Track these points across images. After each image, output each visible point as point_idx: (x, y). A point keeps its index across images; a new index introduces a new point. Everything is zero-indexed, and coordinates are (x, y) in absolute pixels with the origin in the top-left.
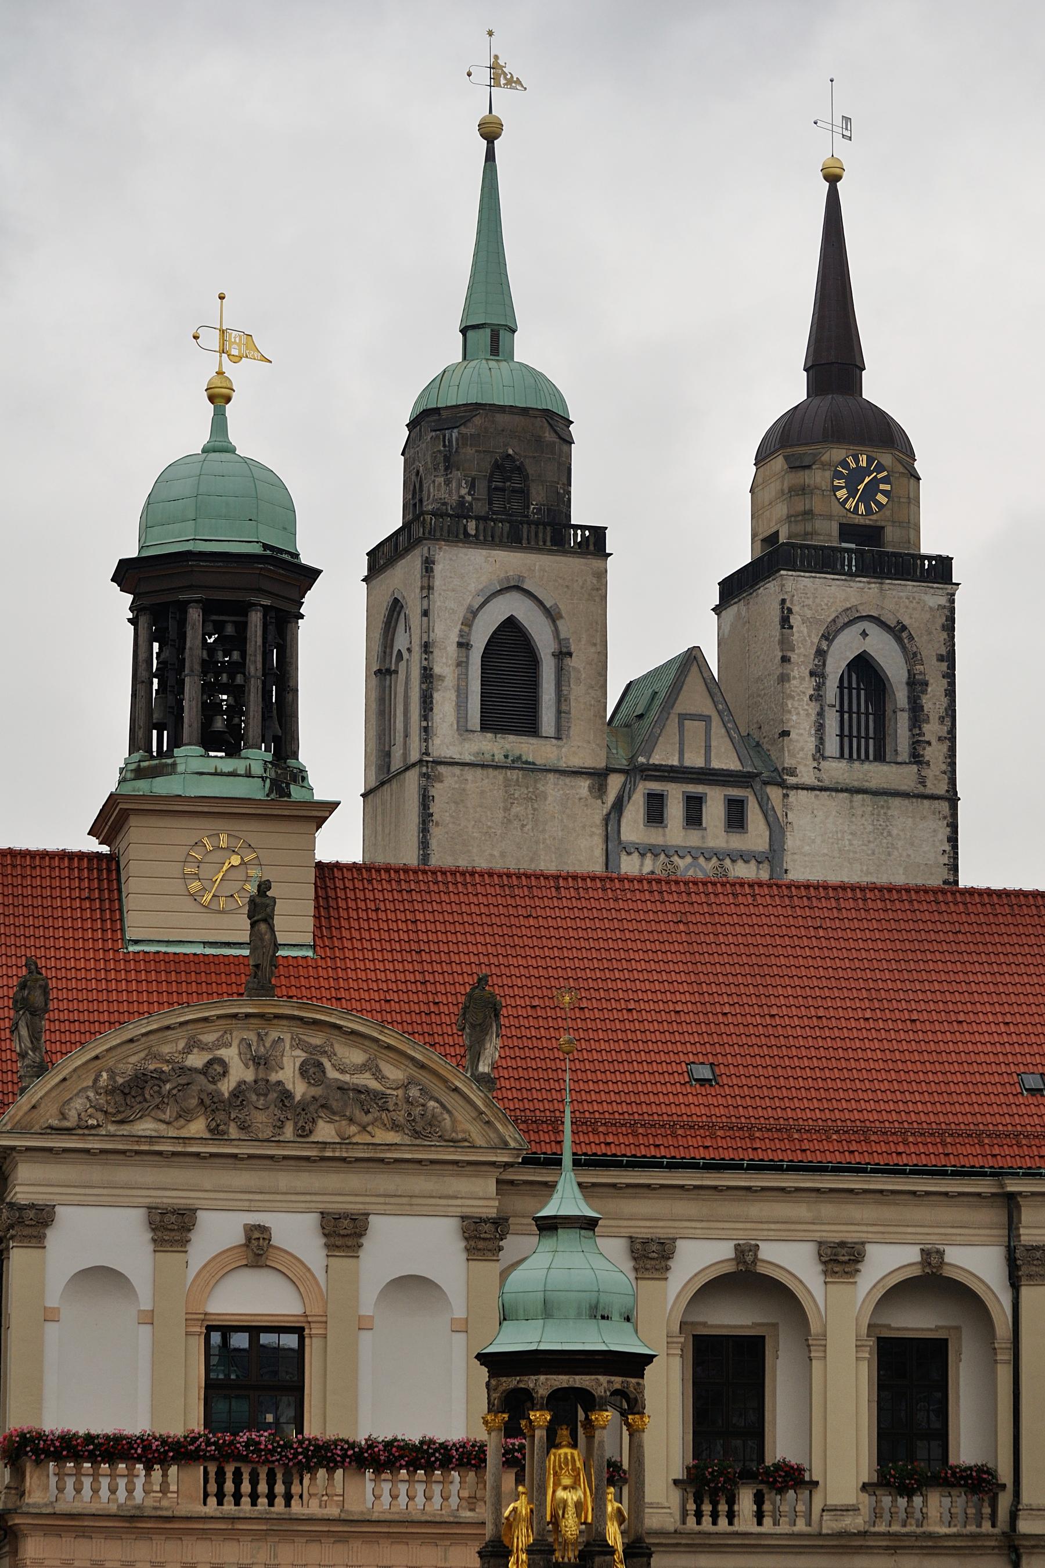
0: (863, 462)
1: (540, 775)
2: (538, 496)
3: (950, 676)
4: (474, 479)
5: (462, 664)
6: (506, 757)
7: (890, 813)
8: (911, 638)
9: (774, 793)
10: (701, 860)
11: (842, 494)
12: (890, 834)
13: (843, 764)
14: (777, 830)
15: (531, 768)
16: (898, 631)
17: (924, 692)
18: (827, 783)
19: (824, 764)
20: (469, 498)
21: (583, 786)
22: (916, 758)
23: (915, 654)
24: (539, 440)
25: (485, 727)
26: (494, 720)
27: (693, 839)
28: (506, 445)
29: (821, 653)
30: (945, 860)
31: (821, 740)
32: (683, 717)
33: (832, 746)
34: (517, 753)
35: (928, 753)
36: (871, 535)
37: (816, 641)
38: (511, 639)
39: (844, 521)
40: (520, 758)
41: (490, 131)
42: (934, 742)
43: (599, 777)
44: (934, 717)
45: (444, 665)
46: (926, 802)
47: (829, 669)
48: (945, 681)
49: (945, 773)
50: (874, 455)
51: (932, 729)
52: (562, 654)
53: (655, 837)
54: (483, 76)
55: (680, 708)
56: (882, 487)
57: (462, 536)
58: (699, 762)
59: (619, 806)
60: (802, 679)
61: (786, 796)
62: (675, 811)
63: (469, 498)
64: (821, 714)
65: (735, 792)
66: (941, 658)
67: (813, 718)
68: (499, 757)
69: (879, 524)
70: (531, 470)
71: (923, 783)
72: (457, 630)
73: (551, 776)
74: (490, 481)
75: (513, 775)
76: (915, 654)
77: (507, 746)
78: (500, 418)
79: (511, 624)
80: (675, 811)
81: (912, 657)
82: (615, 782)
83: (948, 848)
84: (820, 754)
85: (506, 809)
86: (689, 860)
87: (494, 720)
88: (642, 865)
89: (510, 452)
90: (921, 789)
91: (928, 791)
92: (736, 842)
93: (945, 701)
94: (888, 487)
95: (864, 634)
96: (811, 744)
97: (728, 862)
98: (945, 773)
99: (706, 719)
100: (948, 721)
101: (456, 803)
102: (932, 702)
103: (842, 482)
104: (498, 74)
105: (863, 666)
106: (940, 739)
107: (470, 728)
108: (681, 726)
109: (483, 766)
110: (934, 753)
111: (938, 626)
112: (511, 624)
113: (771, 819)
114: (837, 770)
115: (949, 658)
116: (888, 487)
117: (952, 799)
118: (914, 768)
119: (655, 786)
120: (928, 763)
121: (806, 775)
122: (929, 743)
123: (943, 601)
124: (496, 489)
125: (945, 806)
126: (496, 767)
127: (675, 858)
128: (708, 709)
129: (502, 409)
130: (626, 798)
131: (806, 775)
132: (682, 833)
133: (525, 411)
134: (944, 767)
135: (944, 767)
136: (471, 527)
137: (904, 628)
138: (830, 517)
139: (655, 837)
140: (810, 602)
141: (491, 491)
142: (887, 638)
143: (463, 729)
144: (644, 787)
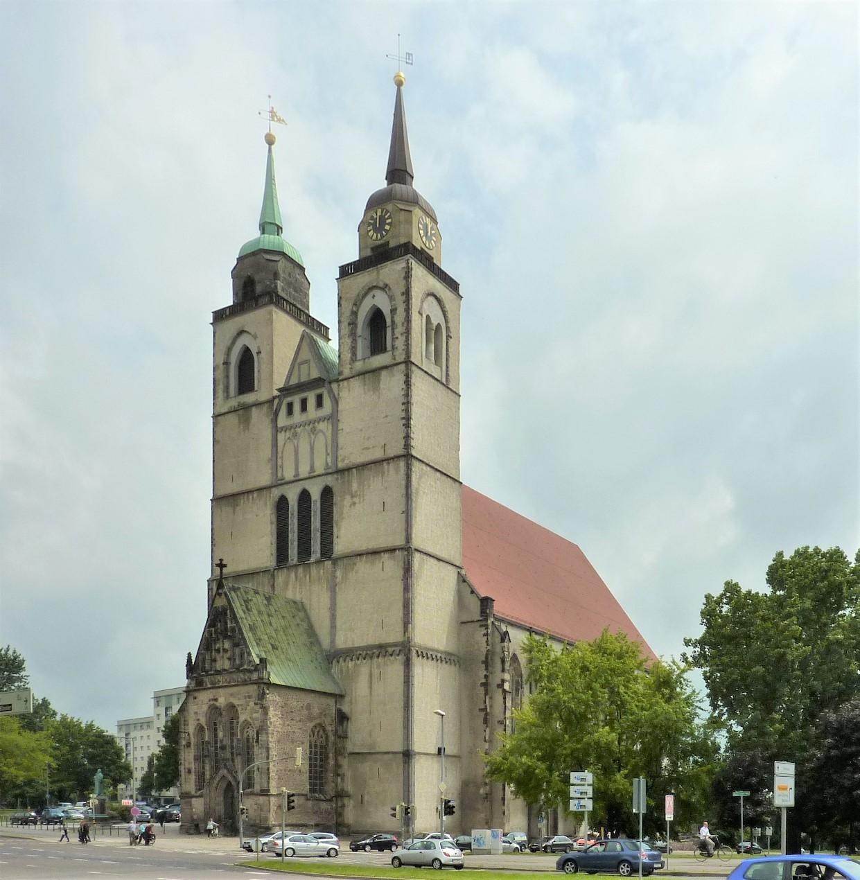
14: (336, 401)
22: (393, 348)
30: (403, 393)
31: (354, 354)
41: (270, 141)
42: (399, 337)
43: (271, 401)
52: (259, 353)
54: (268, 115)
59: (276, 414)
62: (297, 407)
65: (319, 391)
80: (297, 407)
82: (276, 402)
86: (302, 427)
88: (285, 436)
104: (273, 115)
106: (402, 334)
108: (299, 368)
110: (400, 343)
114: (359, 366)
121: (347, 373)
122: (397, 338)
132: (315, 412)
135: (403, 347)
139: (290, 422)
143: (227, 397)
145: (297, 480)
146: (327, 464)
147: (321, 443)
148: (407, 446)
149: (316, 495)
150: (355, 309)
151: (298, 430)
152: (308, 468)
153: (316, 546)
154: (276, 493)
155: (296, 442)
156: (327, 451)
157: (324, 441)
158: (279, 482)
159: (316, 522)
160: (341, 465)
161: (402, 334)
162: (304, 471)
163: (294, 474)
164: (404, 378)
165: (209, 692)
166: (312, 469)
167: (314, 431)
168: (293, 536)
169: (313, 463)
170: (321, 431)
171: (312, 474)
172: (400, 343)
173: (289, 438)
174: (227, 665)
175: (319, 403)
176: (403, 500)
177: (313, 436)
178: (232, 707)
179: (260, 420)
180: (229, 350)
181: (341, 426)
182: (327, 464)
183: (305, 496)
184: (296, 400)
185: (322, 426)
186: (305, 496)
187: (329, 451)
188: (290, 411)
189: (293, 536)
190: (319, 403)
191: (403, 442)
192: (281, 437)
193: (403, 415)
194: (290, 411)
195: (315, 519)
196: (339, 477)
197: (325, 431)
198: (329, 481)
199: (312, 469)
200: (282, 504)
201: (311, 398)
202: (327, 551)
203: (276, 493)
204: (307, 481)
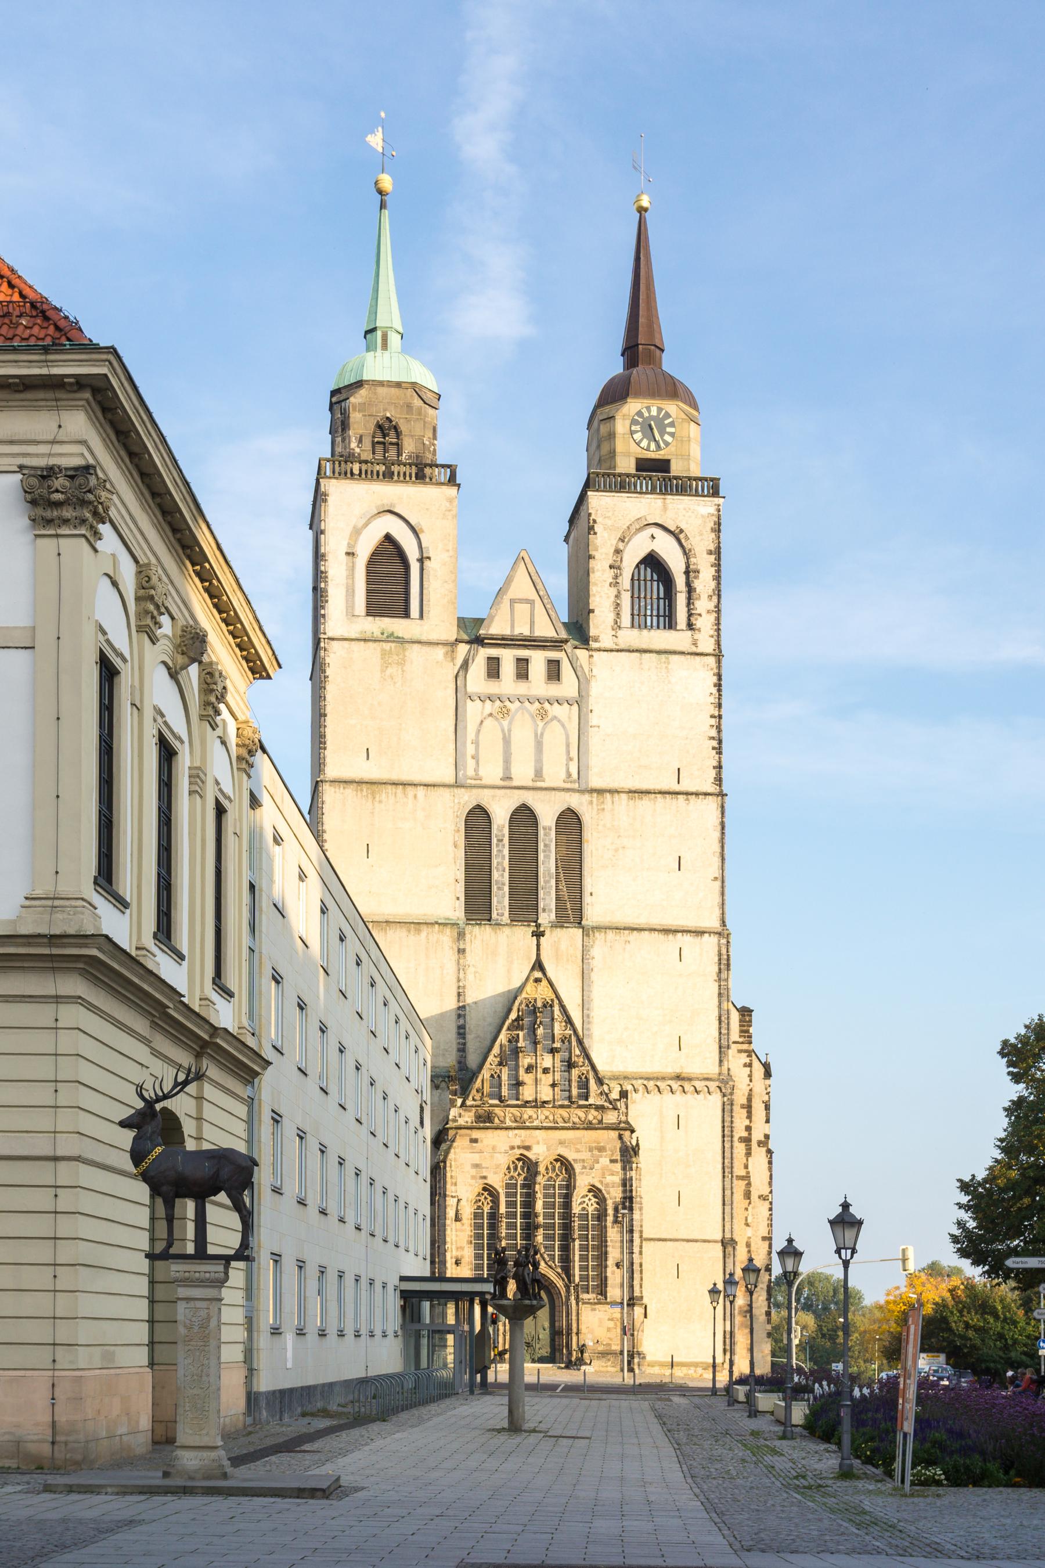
0: (654, 412)
1: (407, 645)
2: (409, 447)
3: (718, 565)
4: (361, 437)
5: (352, 569)
6: (382, 634)
7: (670, 667)
8: (687, 538)
9: (582, 654)
10: (527, 703)
11: (638, 436)
12: (669, 682)
13: (636, 631)
14: (583, 681)
15: (401, 641)
16: (676, 535)
17: (696, 577)
18: (622, 646)
19: (620, 633)
20: (357, 450)
21: (440, 652)
22: (690, 626)
23: (690, 550)
24: (409, 407)
25: (369, 613)
26: (374, 609)
27: (522, 688)
28: (385, 410)
29: (618, 551)
32: (513, 601)
33: (626, 619)
34: (390, 631)
35: (699, 623)
36: (663, 466)
37: (614, 542)
38: (390, 550)
39: (640, 456)
40: (392, 634)
42: (704, 614)
44: (704, 597)
45: (336, 568)
46: (697, 658)
47: (625, 564)
48: (713, 569)
49: (712, 636)
50: (662, 406)
51: (704, 605)
53: (492, 687)
55: (512, 593)
56: (669, 430)
57: (349, 475)
58: (526, 632)
59: (465, 665)
60: (604, 571)
61: (591, 656)
62: (508, 668)
63: (357, 450)
64: (618, 596)
66: (710, 553)
67: (612, 599)
68: (377, 634)
69: (666, 457)
70: (403, 427)
71: (695, 644)
72: (345, 543)
73: (416, 646)
74: (374, 437)
75: (387, 646)
76: (690, 550)
77: (383, 626)
78: (380, 390)
79: (388, 538)
80: (508, 668)
81: (686, 553)
83: (714, 690)
84: (617, 626)
85: (383, 671)
87: (374, 609)
89: (388, 415)
90: (694, 649)
91: (699, 650)
92: (554, 690)
93: (713, 584)
94: (672, 430)
95: (653, 537)
96: (612, 616)
97: (547, 705)
98: (712, 636)
99: (532, 603)
100: (715, 599)
101: (345, 668)
102: (704, 583)
103: (638, 428)
105: (653, 562)
106: (708, 612)
107: (356, 613)
109: (365, 640)
110: (705, 623)
111: (709, 529)
112: (388, 538)
113: (579, 674)
115: (717, 552)
116: (672, 430)
117: (718, 656)
118: (689, 633)
119: (494, 652)
120: (699, 630)
121: (606, 641)
122: (700, 615)
123: (712, 510)
124: (378, 443)
125: (712, 660)
126: (375, 641)
127: (507, 703)
128: (532, 595)
129: (381, 383)
130: (470, 661)
131: (606, 641)
133: (398, 385)
134: (712, 632)
136: (356, 468)
137: (682, 531)
138: (627, 454)
140: (610, 514)
141: (374, 444)
142: (671, 540)
143: (351, 615)
144: (484, 653)
145: (507, 783)
146: (569, 775)
147: (556, 741)
148: (719, 780)
149: (547, 817)
150: (621, 546)
151: (513, 707)
152: (531, 773)
153: (547, 899)
154: (468, 799)
155: (505, 723)
156: (568, 752)
157: (564, 737)
158: (469, 781)
159: (548, 863)
160: (595, 782)
161: (708, 612)
162: (522, 773)
163: (501, 775)
164: (715, 679)
165: (511, 1133)
166: (539, 774)
167: (543, 714)
168: (501, 876)
169: (541, 769)
170: (555, 718)
171: (539, 784)
172: (705, 623)
173: (491, 715)
174: (546, 1094)
175: (554, 671)
176: (716, 861)
177: (541, 724)
178: (565, 1164)
179: (430, 671)
180: (357, 532)
181: (594, 719)
182: (569, 775)
183: (524, 818)
184: (508, 657)
185: (555, 710)
186: (524, 818)
187: (574, 754)
188: (493, 669)
189: (501, 876)
190: (554, 671)
191: (713, 773)
192: (473, 711)
193: (713, 733)
194: (493, 669)
195: (547, 857)
196: (595, 800)
197: (564, 720)
198: (576, 801)
199: (539, 774)
200: (478, 820)
201: (538, 660)
202: (572, 911)
203: (466, 798)
204: (531, 792)
